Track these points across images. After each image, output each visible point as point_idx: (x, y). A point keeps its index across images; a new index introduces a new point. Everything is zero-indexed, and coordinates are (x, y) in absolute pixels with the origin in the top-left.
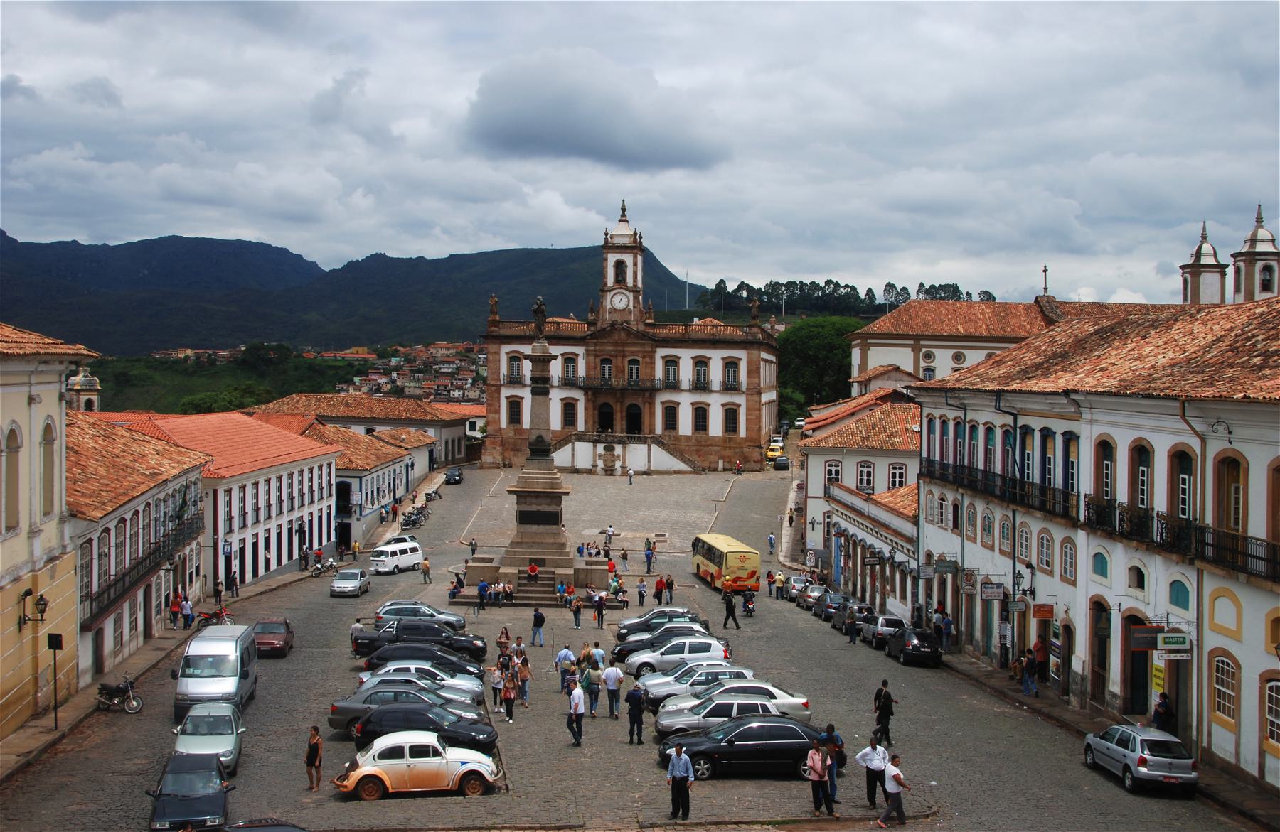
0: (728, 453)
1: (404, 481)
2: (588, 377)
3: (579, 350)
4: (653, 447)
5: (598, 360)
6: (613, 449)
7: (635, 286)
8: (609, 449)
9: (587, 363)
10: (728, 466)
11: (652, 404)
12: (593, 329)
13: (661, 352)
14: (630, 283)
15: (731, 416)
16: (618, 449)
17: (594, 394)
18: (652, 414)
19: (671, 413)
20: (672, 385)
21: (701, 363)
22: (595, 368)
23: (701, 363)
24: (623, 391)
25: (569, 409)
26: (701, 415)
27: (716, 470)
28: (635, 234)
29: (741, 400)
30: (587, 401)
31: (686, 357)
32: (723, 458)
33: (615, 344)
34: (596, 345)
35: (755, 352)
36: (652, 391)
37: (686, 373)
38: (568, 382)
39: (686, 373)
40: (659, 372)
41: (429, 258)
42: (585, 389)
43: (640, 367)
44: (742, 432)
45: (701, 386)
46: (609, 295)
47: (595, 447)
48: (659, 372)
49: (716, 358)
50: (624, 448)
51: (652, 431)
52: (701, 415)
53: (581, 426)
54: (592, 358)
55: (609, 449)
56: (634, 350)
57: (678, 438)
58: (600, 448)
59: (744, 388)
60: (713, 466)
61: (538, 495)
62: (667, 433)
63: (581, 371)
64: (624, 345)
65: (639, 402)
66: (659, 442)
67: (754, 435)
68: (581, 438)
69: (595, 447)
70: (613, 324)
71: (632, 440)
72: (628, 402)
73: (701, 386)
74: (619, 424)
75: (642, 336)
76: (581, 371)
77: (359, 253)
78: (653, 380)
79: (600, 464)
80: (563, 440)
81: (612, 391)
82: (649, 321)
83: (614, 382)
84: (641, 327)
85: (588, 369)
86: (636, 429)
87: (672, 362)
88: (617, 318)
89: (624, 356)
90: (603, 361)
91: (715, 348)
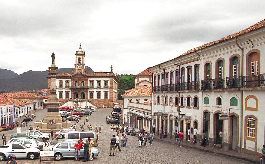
0: (105, 103)
1: (27, 111)
2: (72, 86)
3: (70, 80)
4: (87, 102)
5: (74, 82)
6: (78, 103)
7: (83, 64)
8: (77, 103)
9: (72, 83)
10: (105, 106)
11: (87, 92)
12: (73, 74)
13: (89, 79)
14: (82, 63)
15: (106, 94)
16: (79, 103)
17: (73, 90)
18: (87, 95)
19: (92, 94)
20: (93, 88)
21: (99, 82)
22: (74, 84)
23: (99, 82)
24: (80, 89)
25: (67, 94)
26: (99, 94)
27: (102, 107)
28: (83, 51)
29: (108, 90)
30: (72, 92)
31: (95, 80)
32: (104, 104)
33: (78, 78)
34: (74, 78)
35: (112, 79)
36: (87, 89)
37: (95, 84)
38: (67, 87)
39: (95, 84)
40: (89, 84)
41: (41, 71)
42: (70, 89)
43: (84, 83)
44: (109, 98)
45: (99, 87)
46: (77, 66)
47: (73, 102)
48: (89, 84)
49: (102, 80)
50: (80, 102)
51: (87, 98)
52: (99, 94)
53: (70, 97)
54: (73, 81)
55: (77, 103)
56: (83, 79)
57: (93, 100)
58: (75, 103)
59: (109, 88)
60: (102, 106)
61: (52, 104)
62: (91, 99)
63: (70, 85)
64: (80, 78)
65: (84, 92)
66: (88, 101)
67: (111, 99)
68: (70, 101)
69: (73, 102)
70: (78, 74)
71: (82, 101)
72: (81, 92)
73: (99, 87)
74: (79, 97)
75: (85, 76)
76: (70, 85)
77: (26, 70)
78: (87, 86)
79: (75, 107)
80: (66, 102)
81: (77, 89)
82: (86, 72)
83: (78, 87)
84: (84, 74)
85: (72, 84)
86: (84, 98)
87: (92, 82)
88: (79, 71)
89: (80, 81)
90: (75, 82)
91: (102, 78)
